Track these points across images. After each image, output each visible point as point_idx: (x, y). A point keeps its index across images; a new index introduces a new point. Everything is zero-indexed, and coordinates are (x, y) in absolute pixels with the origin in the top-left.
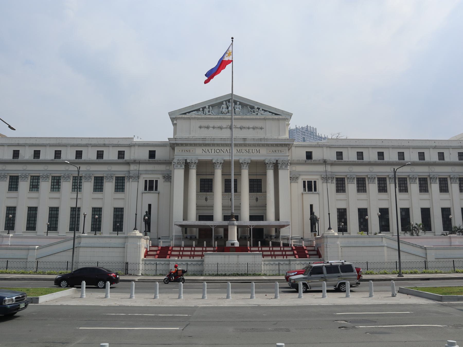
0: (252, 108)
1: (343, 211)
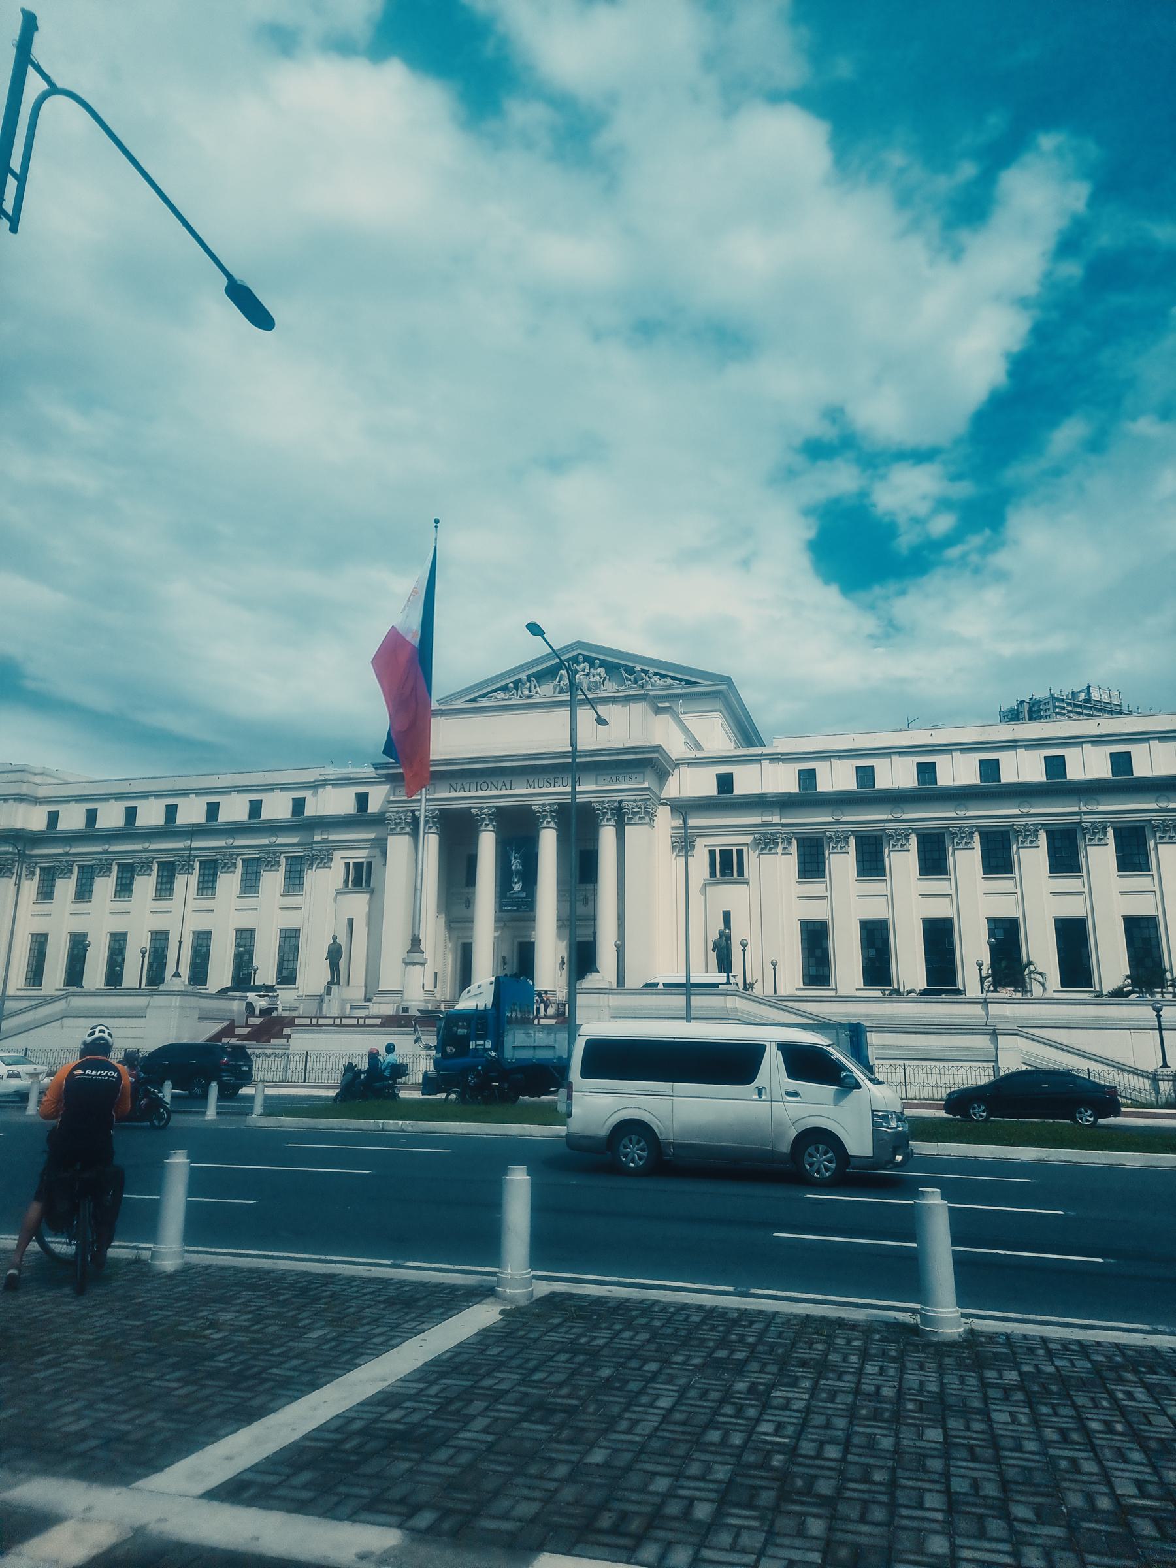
0: (630, 671)
1: (818, 927)
